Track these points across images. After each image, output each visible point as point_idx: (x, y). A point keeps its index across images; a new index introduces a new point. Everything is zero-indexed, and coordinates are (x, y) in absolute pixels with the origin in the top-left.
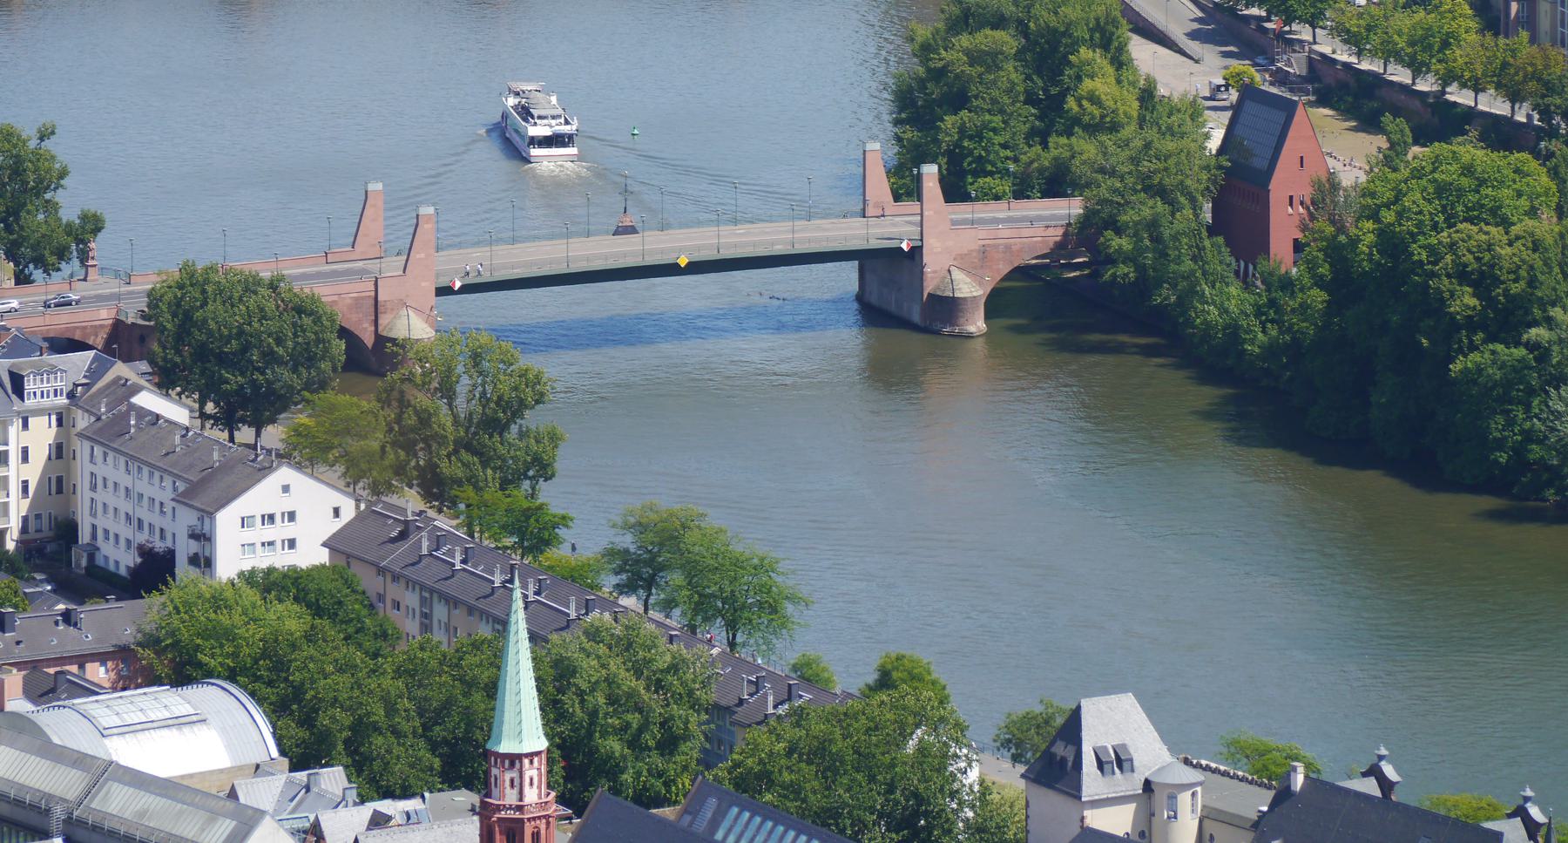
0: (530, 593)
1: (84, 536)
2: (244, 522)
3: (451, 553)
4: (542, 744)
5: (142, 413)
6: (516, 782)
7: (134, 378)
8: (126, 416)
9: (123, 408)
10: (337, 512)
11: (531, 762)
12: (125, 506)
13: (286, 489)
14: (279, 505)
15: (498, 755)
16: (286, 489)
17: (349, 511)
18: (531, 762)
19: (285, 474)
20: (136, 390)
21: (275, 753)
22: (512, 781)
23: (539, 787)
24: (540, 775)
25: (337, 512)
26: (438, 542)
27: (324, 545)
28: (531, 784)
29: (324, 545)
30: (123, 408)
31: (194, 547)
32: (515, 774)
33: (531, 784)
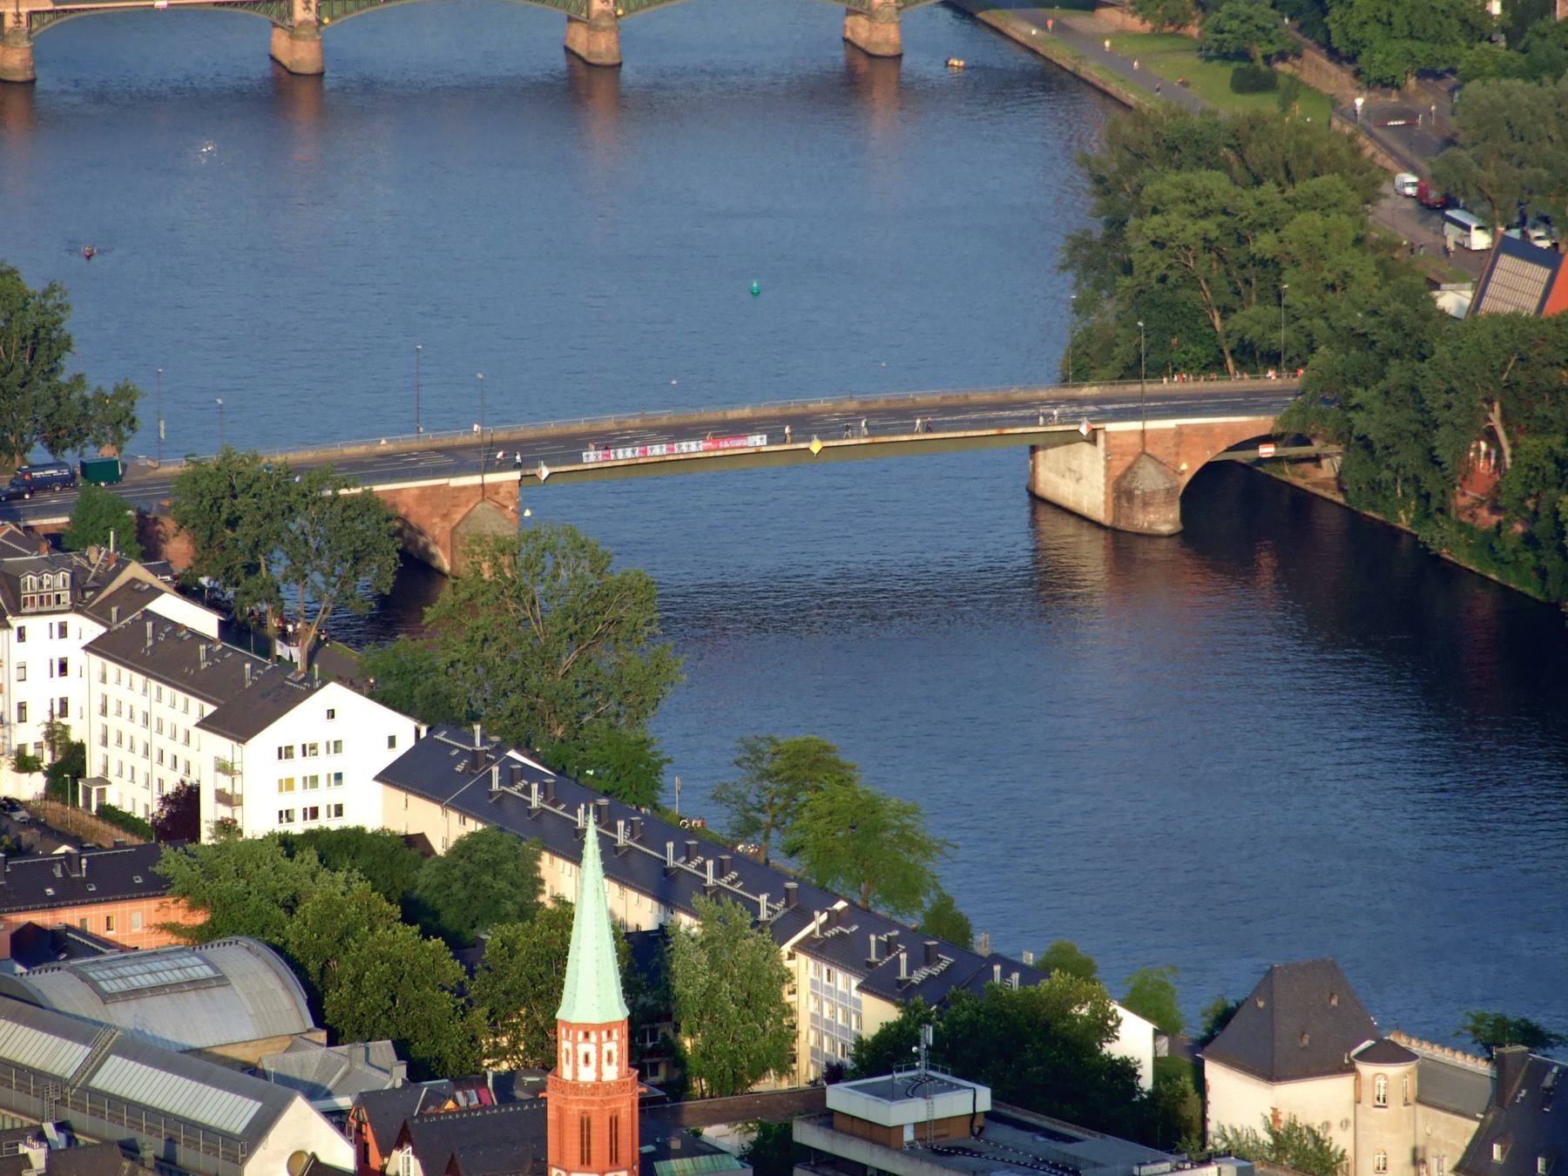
0: (622, 838)
1: (93, 769)
2: (285, 753)
3: (527, 790)
4: (617, 1011)
5: (160, 621)
6: (593, 1058)
7: (162, 586)
8: (138, 626)
9: (137, 615)
10: (392, 742)
11: (609, 1034)
12: (141, 735)
13: (331, 714)
14: (323, 733)
15: (569, 1026)
16: (331, 714)
17: (406, 743)
18: (609, 1034)
19: (334, 694)
20: (155, 593)
21: (310, 1024)
22: (587, 1057)
23: (619, 1064)
24: (620, 1050)
25: (392, 742)
26: (510, 776)
27: (378, 778)
28: (610, 1060)
29: (378, 778)
30: (137, 615)
31: (224, 782)
32: (590, 1048)
33: (610, 1060)
